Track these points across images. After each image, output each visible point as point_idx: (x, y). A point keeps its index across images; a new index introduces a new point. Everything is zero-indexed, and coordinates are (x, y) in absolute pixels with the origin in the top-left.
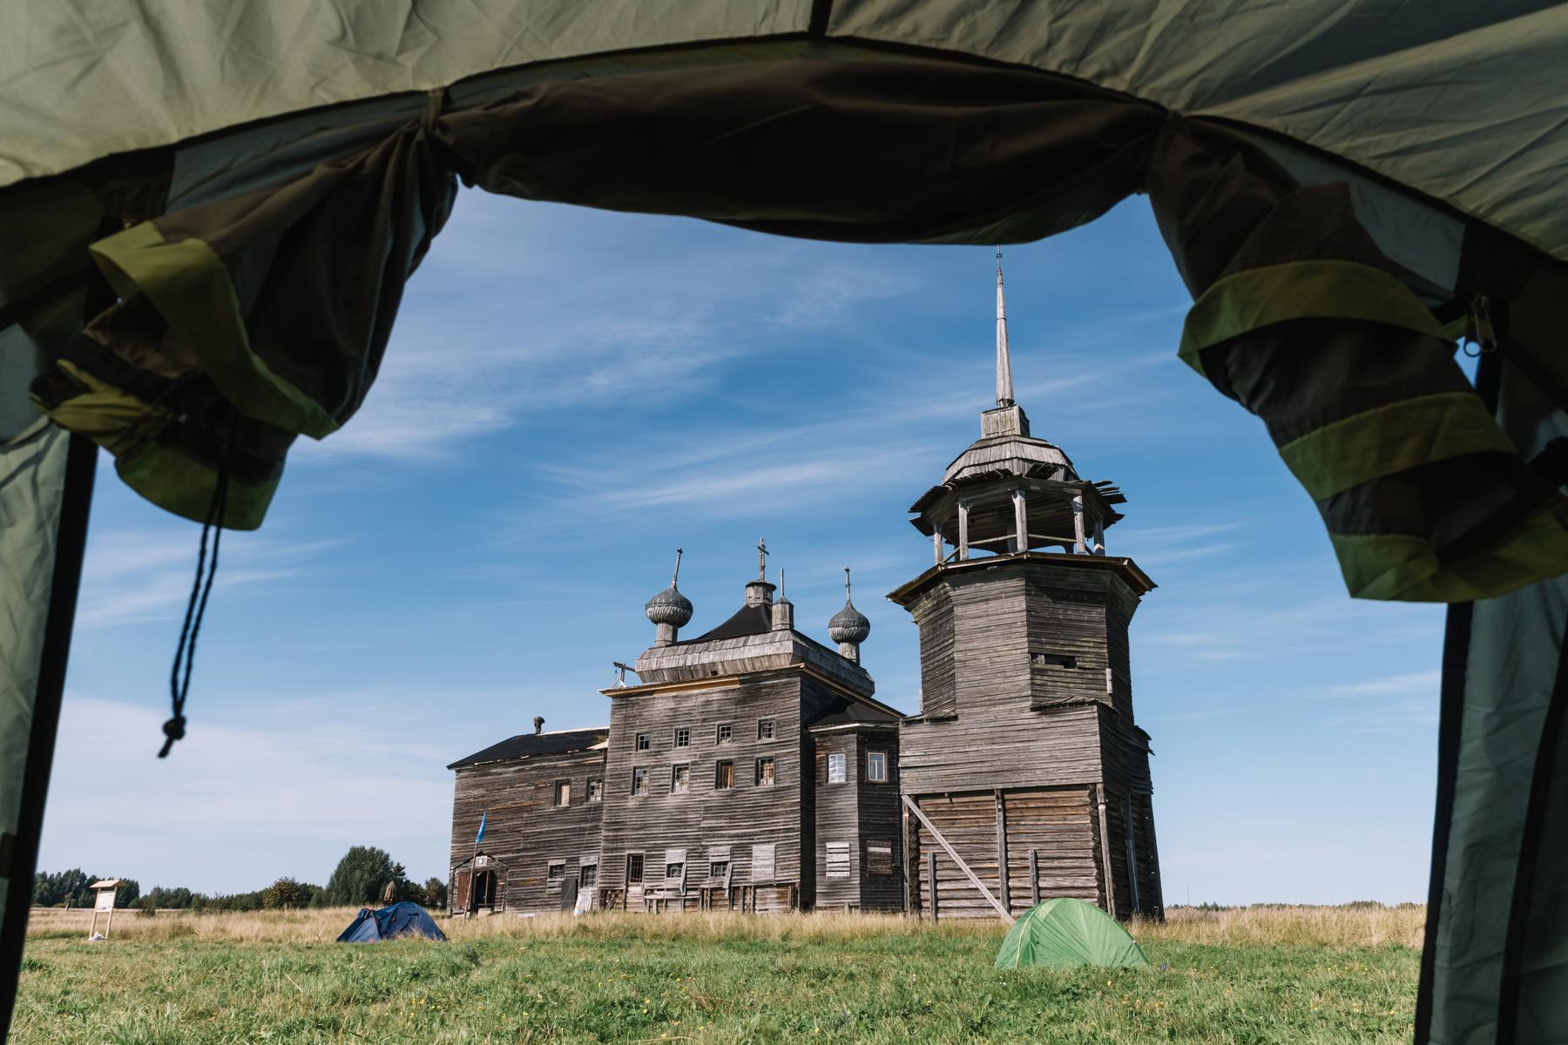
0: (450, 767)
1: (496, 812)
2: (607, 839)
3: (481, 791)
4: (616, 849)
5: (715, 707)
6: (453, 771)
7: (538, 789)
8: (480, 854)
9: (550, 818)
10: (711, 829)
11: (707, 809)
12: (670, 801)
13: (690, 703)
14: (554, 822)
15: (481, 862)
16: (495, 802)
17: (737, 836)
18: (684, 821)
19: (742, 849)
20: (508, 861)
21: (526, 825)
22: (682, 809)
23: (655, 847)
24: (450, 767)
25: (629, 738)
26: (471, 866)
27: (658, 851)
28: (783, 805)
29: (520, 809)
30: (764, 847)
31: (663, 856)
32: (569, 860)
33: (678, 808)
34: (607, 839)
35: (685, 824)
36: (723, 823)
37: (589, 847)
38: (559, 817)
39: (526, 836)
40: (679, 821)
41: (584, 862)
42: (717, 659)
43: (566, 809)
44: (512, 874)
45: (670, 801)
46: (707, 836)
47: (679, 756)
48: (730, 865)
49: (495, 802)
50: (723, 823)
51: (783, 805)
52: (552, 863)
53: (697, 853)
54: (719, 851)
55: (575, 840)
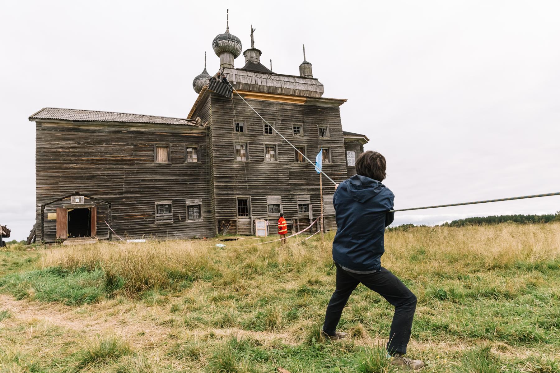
0: (31, 119)
1: (93, 162)
2: (218, 187)
3: (72, 144)
4: (228, 194)
5: (289, 113)
6: (34, 123)
7: (137, 148)
8: (77, 194)
9: (154, 170)
10: (295, 185)
11: (291, 173)
12: (264, 167)
13: (272, 108)
14: (157, 173)
15: (78, 201)
16: (89, 154)
17: (313, 190)
18: (277, 179)
19: (316, 197)
20: (110, 202)
21: (127, 174)
22: (275, 172)
23: (258, 194)
24: (31, 119)
25: (229, 123)
26: (65, 204)
27: (259, 197)
28: (338, 175)
29: (122, 162)
30: (328, 196)
31: (265, 200)
32: (174, 201)
33: (272, 171)
34: (218, 187)
35: (277, 180)
36: (303, 182)
37: (192, 193)
38: (160, 170)
39: (129, 183)
40: (273, 181)
41: (188, 202)
42: (279, 85)
43: (167, 166)
44: (117, 210)
45: (264, 167)
46: (294, 189)
47: (267, 140)
48: (311, 206)
49: (89, 154)
50: (303, 182)
51: (338, 175)
52: (156, 203)
53: (288, 198)
54: (303, 198)
55: (181, 188)
